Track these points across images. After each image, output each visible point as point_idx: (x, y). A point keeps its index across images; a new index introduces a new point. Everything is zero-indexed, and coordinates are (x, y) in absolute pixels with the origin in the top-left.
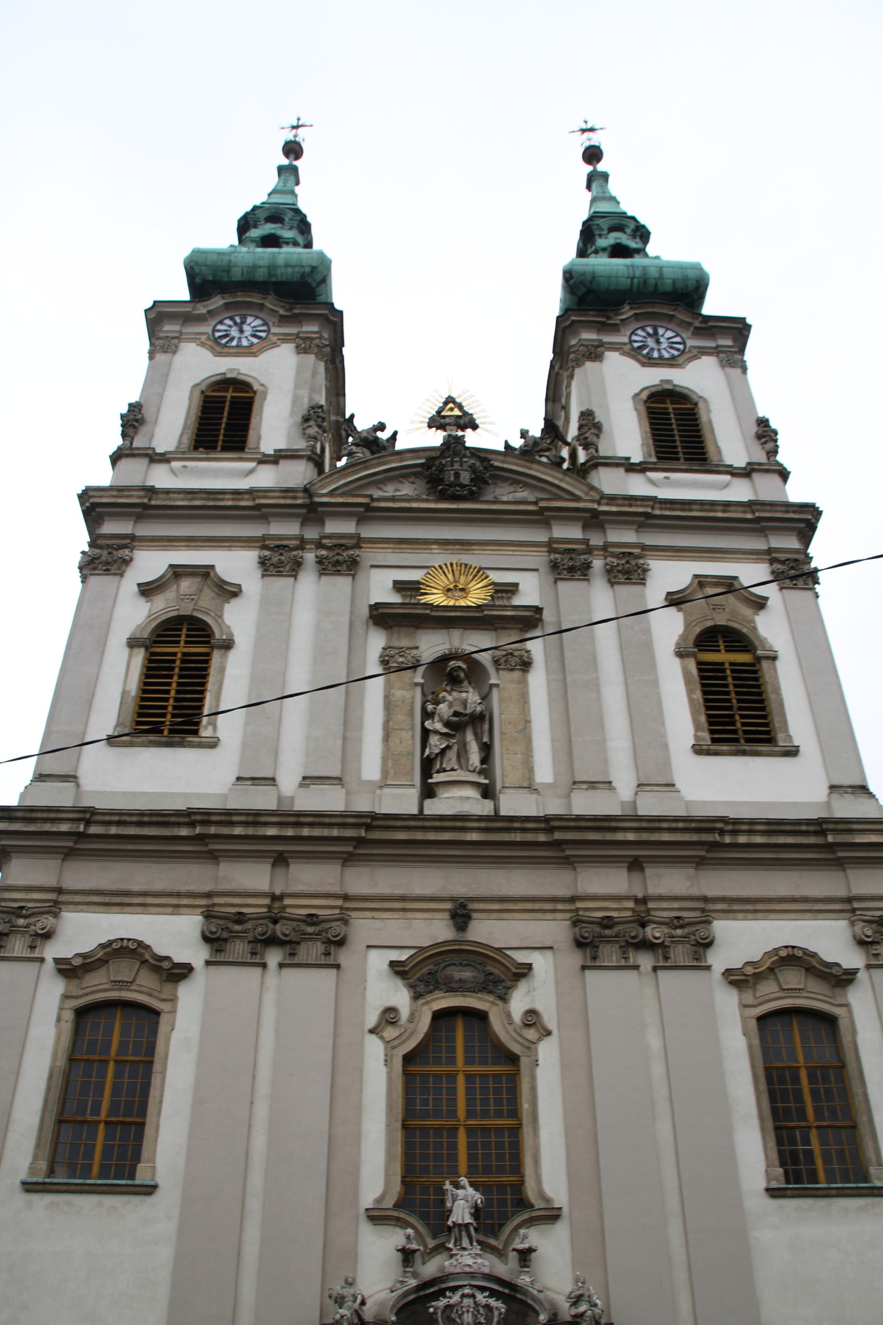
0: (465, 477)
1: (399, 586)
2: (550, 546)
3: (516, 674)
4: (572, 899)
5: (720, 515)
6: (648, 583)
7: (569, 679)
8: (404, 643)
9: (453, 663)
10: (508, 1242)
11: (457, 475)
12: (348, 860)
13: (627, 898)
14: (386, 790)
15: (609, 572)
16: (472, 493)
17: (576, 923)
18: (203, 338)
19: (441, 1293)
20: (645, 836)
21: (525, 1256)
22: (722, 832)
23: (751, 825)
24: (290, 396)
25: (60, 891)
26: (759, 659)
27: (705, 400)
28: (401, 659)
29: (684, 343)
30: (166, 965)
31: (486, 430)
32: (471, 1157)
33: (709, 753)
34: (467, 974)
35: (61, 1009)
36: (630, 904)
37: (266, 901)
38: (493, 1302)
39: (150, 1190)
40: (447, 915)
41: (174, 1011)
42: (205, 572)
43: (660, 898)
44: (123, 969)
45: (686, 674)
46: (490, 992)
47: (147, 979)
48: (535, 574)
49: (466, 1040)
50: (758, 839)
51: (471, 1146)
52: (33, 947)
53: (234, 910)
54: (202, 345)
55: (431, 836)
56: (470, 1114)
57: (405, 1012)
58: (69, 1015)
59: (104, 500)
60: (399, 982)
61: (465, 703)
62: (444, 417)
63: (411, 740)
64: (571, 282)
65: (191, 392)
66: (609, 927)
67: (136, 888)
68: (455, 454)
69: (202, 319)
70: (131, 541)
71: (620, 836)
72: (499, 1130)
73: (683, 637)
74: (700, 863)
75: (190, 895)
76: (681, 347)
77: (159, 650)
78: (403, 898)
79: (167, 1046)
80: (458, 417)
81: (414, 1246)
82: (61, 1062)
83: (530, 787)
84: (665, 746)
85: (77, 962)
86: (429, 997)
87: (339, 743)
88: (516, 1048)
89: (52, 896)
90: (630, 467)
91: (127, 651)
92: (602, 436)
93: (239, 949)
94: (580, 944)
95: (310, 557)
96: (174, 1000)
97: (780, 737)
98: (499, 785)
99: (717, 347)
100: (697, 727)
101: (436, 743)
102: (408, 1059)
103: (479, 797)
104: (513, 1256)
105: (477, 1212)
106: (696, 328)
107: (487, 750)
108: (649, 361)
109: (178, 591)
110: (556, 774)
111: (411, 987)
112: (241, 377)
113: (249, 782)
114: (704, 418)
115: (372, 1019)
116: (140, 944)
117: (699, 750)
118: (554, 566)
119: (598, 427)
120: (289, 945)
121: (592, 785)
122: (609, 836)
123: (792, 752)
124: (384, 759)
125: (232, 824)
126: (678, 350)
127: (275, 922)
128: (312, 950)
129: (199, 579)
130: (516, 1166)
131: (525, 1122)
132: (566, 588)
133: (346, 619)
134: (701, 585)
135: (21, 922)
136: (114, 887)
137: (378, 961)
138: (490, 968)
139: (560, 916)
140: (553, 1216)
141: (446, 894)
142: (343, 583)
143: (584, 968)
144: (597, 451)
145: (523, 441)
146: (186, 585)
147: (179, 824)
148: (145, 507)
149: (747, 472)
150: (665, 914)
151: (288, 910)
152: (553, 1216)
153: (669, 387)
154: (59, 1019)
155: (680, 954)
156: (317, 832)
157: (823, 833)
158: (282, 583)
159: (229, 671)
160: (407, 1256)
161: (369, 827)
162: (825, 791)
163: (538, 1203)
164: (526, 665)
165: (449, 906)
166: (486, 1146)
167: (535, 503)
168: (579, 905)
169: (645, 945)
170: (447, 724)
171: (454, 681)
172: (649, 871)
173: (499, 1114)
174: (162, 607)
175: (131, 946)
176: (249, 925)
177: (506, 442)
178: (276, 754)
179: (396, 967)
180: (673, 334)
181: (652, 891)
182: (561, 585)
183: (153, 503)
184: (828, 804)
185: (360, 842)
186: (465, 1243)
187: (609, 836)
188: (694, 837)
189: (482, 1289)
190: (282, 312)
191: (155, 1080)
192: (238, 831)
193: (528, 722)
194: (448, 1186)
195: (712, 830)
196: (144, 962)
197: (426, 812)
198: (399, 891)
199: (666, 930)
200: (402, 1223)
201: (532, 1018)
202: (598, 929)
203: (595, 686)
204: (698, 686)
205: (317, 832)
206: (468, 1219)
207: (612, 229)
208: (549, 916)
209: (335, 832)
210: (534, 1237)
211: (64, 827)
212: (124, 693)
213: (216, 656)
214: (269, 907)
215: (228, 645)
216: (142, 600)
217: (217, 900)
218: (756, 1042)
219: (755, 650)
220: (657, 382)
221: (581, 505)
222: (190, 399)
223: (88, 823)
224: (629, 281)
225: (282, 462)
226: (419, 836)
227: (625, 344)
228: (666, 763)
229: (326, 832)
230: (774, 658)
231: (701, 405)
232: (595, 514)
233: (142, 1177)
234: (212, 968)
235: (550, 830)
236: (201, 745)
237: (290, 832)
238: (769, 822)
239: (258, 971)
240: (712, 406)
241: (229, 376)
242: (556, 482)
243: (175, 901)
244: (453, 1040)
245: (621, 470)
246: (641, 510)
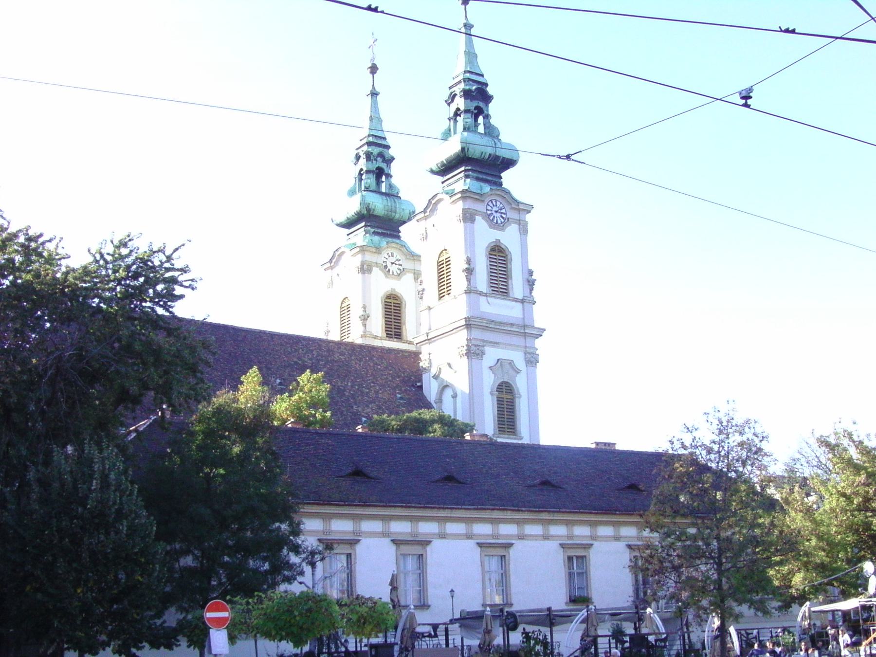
76: (504, 216)
90: (481, 294)
108: (494, 224)
149: (522, 301)
230: (520, 397)
231: (509, 257)
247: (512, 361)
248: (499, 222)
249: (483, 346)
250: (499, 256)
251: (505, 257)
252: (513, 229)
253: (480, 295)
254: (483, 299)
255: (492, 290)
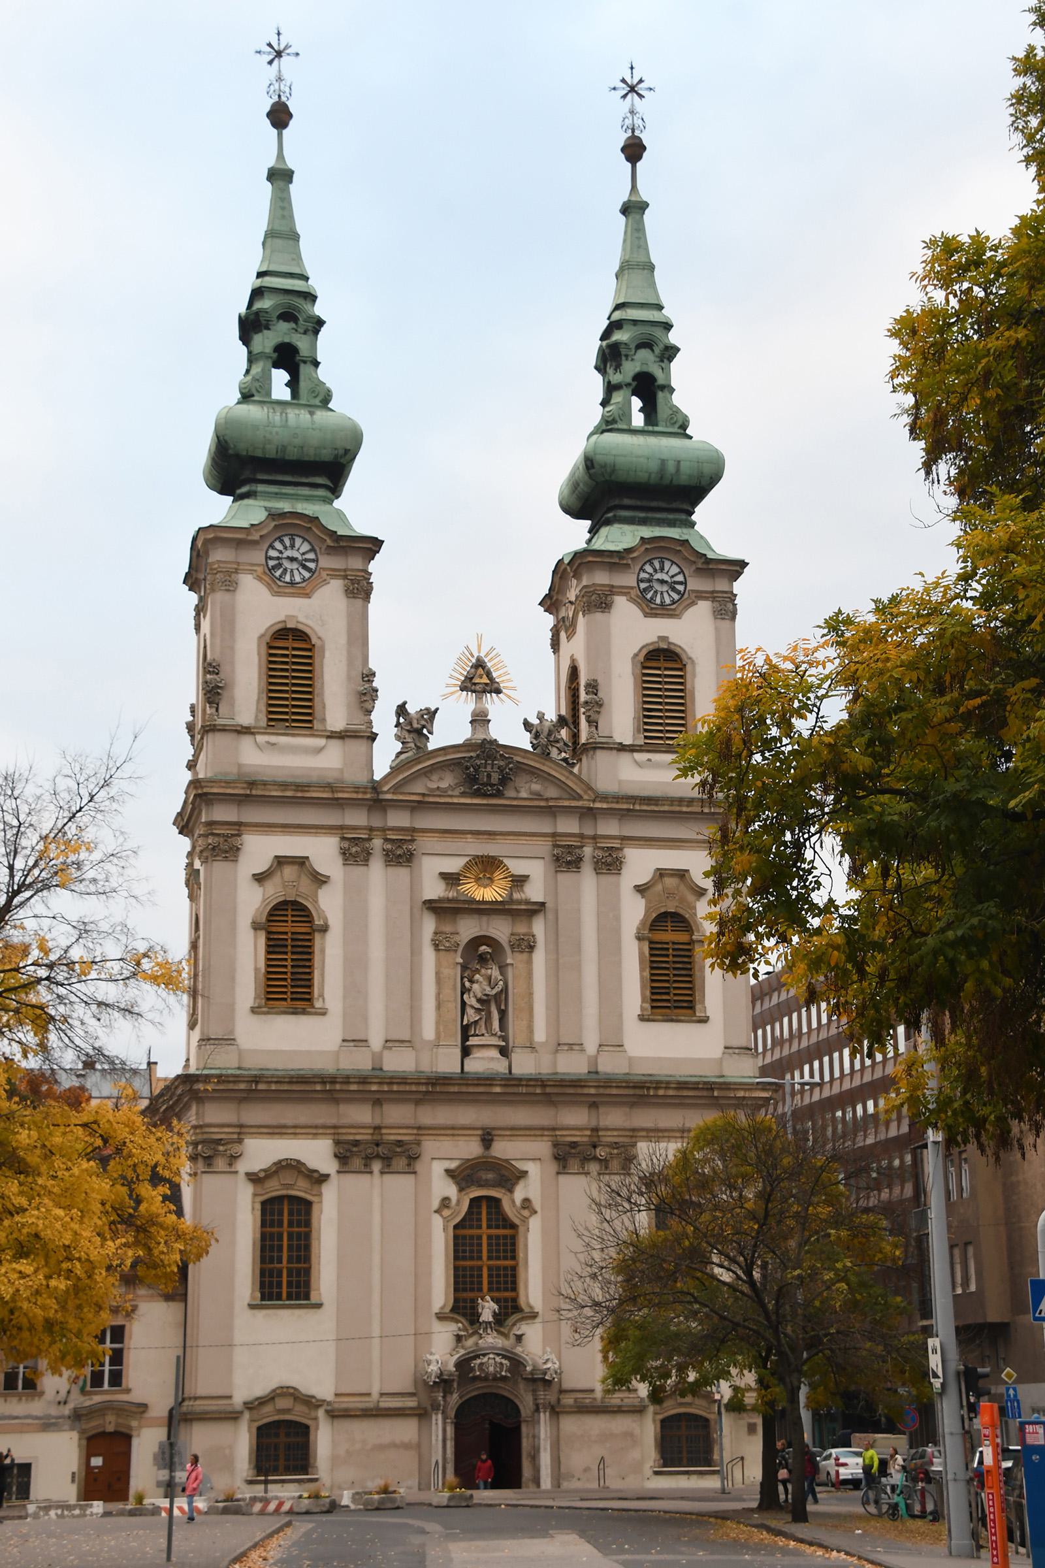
0: (495, 778)
1: (445, 876)
2: (554, 835)
3: (525, 956)
4: (554, 1129)
5: (684, 809)
6: (623, 871)
7: (561, 961)
8: (448, 928)
9: (483, 948)
10: (510, 1330)
11: (489, 776)
12: (418, 1102)
13: (587, 1129)
14: (441, 1050)
15: (597, 863)
16: (498, 790)
17: (556, 1145)
18: (260, 569)
19: (478, 1357)
20: (601, 1091)
21: (519, 1338)
22: (648, 1088)
23: (667, 1085)
24: (345, 653)
25: (241, 1126)
26: (691, 942)
27: (693, 662)
28: (447, 944)
29: (685, 583)
30: (316, 1175)
31: (509, 697)
32: (490, 1283)
33: (649, 1020)
34: (490, 1176)
35: (253, 1202)
36: (588, 1133)
37: (370, 1131)
38: (504, 1361)
39: (319, 1306)
40: (479, 1138)
41: (321, 1202)
42: (301, 862)
43: (607, 1129)
44: (288, 1178)
45: (641, 954)
46: (503, 1187)
47: (302, 1183)
48: (542, 861)
49: (488, 1213)
50: (671, 1092)
51: (490, 1276)
52: (230, 1165)
53: (351, 1137)
54: (260, 579)
55: (471, 1089)
56: (489, 1258)
57: (454, 1199)
58: (258, 1206)
59: (215, 790)
60: (450, 1181)
61: (489, 978)
62: (475, 684)
63: (454, 1008)
64: (592, 471)
65: (259, 646)
66: (574, 1148)
67: (289, 1122)
68: (489, 757)
69: (255, 543)
70: (239, 827)
71: (586, 1091)
72: (506, 1268)
73: (643, 922)
74: (633, 1105)
75: (324, 1127)
76: (681, 588)
77: (274, 929)
78: (453, 1128)
79: (319, 1223)
80: (486, 684)
81: (462, 1333)
82: (258, 1236)
83: (532, 1047)
84: (621, 1015)
85: (262, 1175)
86: (468, 1190)
87: (409, 1013)
88: (516, 1221)
89: (237, 1130)
90: (622, 748)
91: (252, 931)
92: (602, 710)
93: (357, 1163)
94: (557, 1158)
95: (377, 843)
96: (320, 1195)
97: (698, 1007)
98: (511, 1044)
99: (713, 592)
100: (643, 1001)
101: (471, 1015)
102: (456, 1227)
103: (499, 1056)
104: (512, 1338)
105: (495, 1315)
106: (698, 569)
107: (503, 1014)
108: (653, 609)
109: (282, 877)
110: (548, 1036)
111: (457, 1183)
112: (300, 627)
113: (352, 1044)
114: (688, 686)
115: (436, 1204)
116: (298, 1162)
117: (642, 1018)
118: (557, 859)
119: (600, 704)
120: (387, 1161)
121: (571, 1046)
122: (579, 1091)
123: (705, 1020)
124: (438, 1023)
125: (349, 1083)
126: (678, 592)
127: (377, 1145)
128: (401, 1163)
129: (296, 867)
130: (514, 1289)
131: (521, 1264)
132: (565, 879)
133: (407, 908)
134: (661, 875)
135: (221, 1148)
136: (274, 1122)
137: (438, 1169)
138: (504, 1172)
139: (545, 1138)
140: (534, 1316)
141: (479, 1124)
142: (402, 873)
143: (558, 1173)
144: (597, 727)
145: (538, 721)
146: (289, 872)
147: (315, 1083)
148: (247, 796)
150: (609, 1139)
151: (386, 1137)
152: (534, 1316)
153: (664, 646)
154: (253, 1209)
155: (615, 1165)
156: (402, 1088)
157: (712, 1089)
158: (358, 871)
159: (328, 951)
160: (459, 1338)
161: (433, 1084)
162: (721, 1049)
163: (527, 1310)
164: (531, 948)
165: (479, 1132)
166: (498, 1276)
167: (547, 800)
168: (558, 1133)
169: (595, 1158)
170: (479, 1001)
171: (483, 959)
172: (602, 1110)
173: (505, 1258)
174: (272, 892)
175: (294, 1163)
176: (361, 1147)
177: (525, 720)
178: (365, 1019)
179: (449, 1173)
180: (678, 570)
181: (602, 1124)
182: (561, 876)
183: (254, 792)
184: (720, 1061)
185: (427, 1092)
186: (489, 1331)
187: (579, 1091)
188: (631, 1092)
189: (498, 1355)
190: (329, 542)
191: (314, 1243)
192: (354, 1087)
193: (531, 994)
194: (480, 1301)
195: (643, 1087)
196: (300, 1172)
197: (466, 1069)
198: (450, 1122)
199: (608, 1150)
200: (457, 1321)
201: (527, 1202)
202: (568, 1148)
203: (578, 968)
204: (648, 964)
205: (402, 1088)
206: (491, 1319)
207: (639, 346)
208: (539, 1138)
209: (414, 1088)
210: (524, 1328)
211: (242, 1086)
212: (256, 970)
213: (317, 936)
214: (372, 1134)
215: (324, 929)
216: (256, 884)
217: (341, 1131)
218: (653, 1221)
219: (692, 934)
220: (656, 639)
221: (580, 803)
222: (259, 654)
223: (257, 1083)
224: (646, 475)
225: (348, 741)
226: (464, 1089)
227: (632, 588)
228: (619, 1029)
229: (408, 1088)
231: (689, 668)
232: (591, 809)
233: (314, 1299)
234: (341, 1175)
235: (544, 1086)
236: (316, 1014)
237: (386, 1088)
238: (679, 1083)
239: (369, 1176)
240: (698, 669)
241: (289, 626)
242: (563, 779)
243: (314, 1131)
244: (480, 1213)
245: (615, 752)
246: (625, 806)
247: (687, 871)
248: (668, 601)
249: (621, 849)
250: (666, 669)
251: (680, 669)
252: (700, 613)
253: (619, 750)
254: (625, 758)
255: (646, 737)
